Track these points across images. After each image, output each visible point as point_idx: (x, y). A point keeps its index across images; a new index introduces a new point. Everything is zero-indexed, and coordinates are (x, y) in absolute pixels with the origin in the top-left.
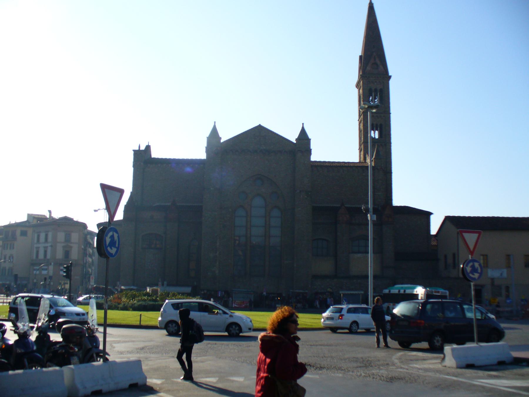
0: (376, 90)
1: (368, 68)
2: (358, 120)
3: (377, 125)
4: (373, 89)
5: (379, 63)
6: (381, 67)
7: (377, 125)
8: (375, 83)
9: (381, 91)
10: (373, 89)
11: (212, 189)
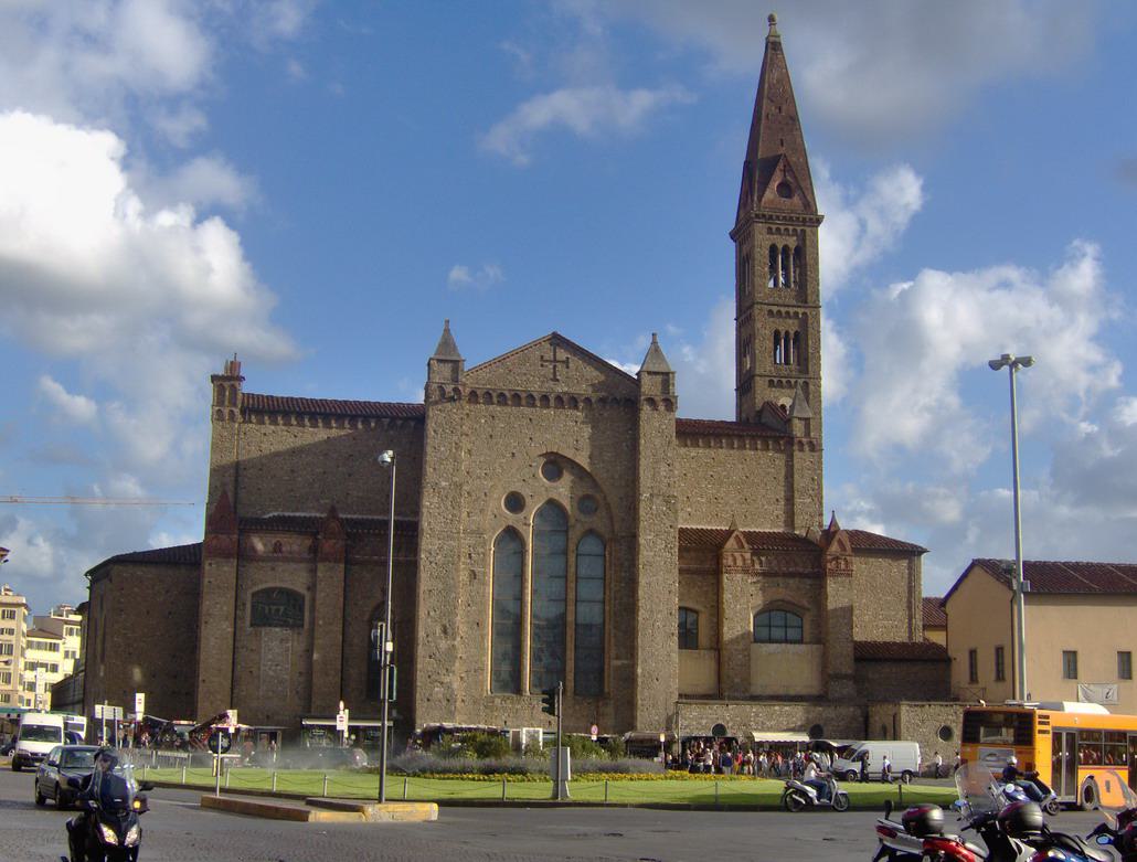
0: (786, 248)
3: (787, 333)
4: (780, 247)
10: (780, 247)
11: (444, 484)
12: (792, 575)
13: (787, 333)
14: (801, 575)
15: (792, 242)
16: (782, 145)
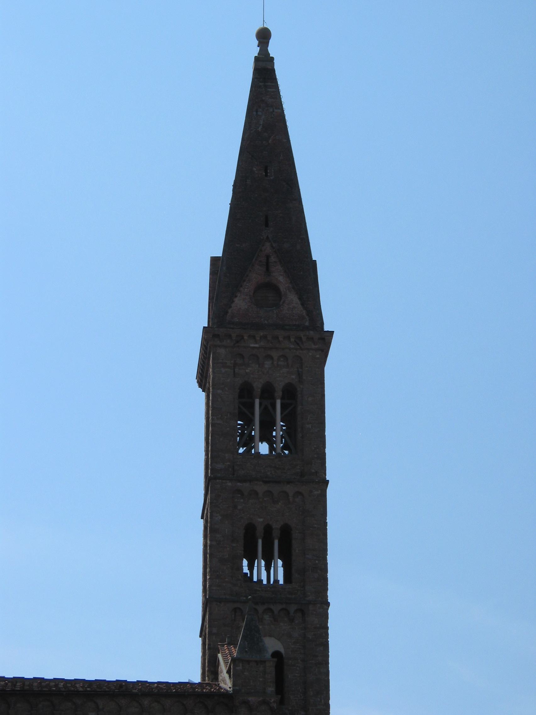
2: (202, 518)
4: (258, 386)
6: (293, 298)
7: (268, 531)
8: (268, 364)
10: (258, 386)
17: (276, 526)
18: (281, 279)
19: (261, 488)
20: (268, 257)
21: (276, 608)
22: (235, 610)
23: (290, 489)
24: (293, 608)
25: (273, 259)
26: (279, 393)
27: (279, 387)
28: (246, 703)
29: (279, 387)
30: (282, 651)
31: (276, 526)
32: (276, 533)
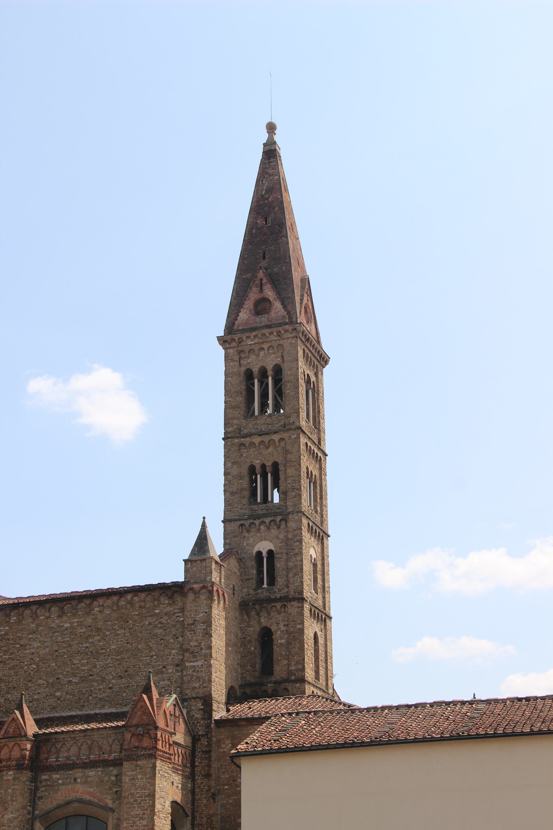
0: (263, 373)
1: (244, 316)
3: (263, 466)
4: (256, 370)
5: (269, 293)
8: (262, 354)
9: (278, 371)
10: (256, 370)
12: (92, 765)
13: (263, 466)
14: (105, 763)
15: (270, 363)
16: (264, 258)
17: (269, 464)
18: (270, 293)
19: (257, 440)
20: (261, 280)
21: (267, 520)
22: (242, 525)
23: (276, 437)
24: (278, 518)
25: (264, 281)
26: (270, 373)
27: (269, 368)
28: (192, 589)
29: (269, 368)
30: (273, 549)
31: (269, 464)
32: (268, 469)
